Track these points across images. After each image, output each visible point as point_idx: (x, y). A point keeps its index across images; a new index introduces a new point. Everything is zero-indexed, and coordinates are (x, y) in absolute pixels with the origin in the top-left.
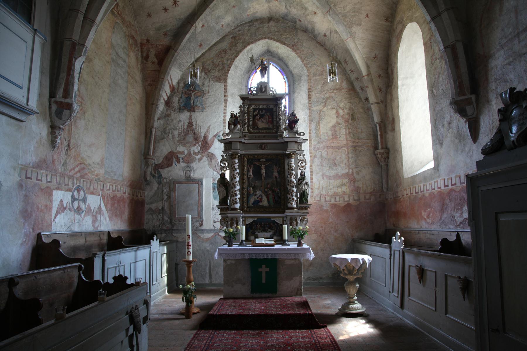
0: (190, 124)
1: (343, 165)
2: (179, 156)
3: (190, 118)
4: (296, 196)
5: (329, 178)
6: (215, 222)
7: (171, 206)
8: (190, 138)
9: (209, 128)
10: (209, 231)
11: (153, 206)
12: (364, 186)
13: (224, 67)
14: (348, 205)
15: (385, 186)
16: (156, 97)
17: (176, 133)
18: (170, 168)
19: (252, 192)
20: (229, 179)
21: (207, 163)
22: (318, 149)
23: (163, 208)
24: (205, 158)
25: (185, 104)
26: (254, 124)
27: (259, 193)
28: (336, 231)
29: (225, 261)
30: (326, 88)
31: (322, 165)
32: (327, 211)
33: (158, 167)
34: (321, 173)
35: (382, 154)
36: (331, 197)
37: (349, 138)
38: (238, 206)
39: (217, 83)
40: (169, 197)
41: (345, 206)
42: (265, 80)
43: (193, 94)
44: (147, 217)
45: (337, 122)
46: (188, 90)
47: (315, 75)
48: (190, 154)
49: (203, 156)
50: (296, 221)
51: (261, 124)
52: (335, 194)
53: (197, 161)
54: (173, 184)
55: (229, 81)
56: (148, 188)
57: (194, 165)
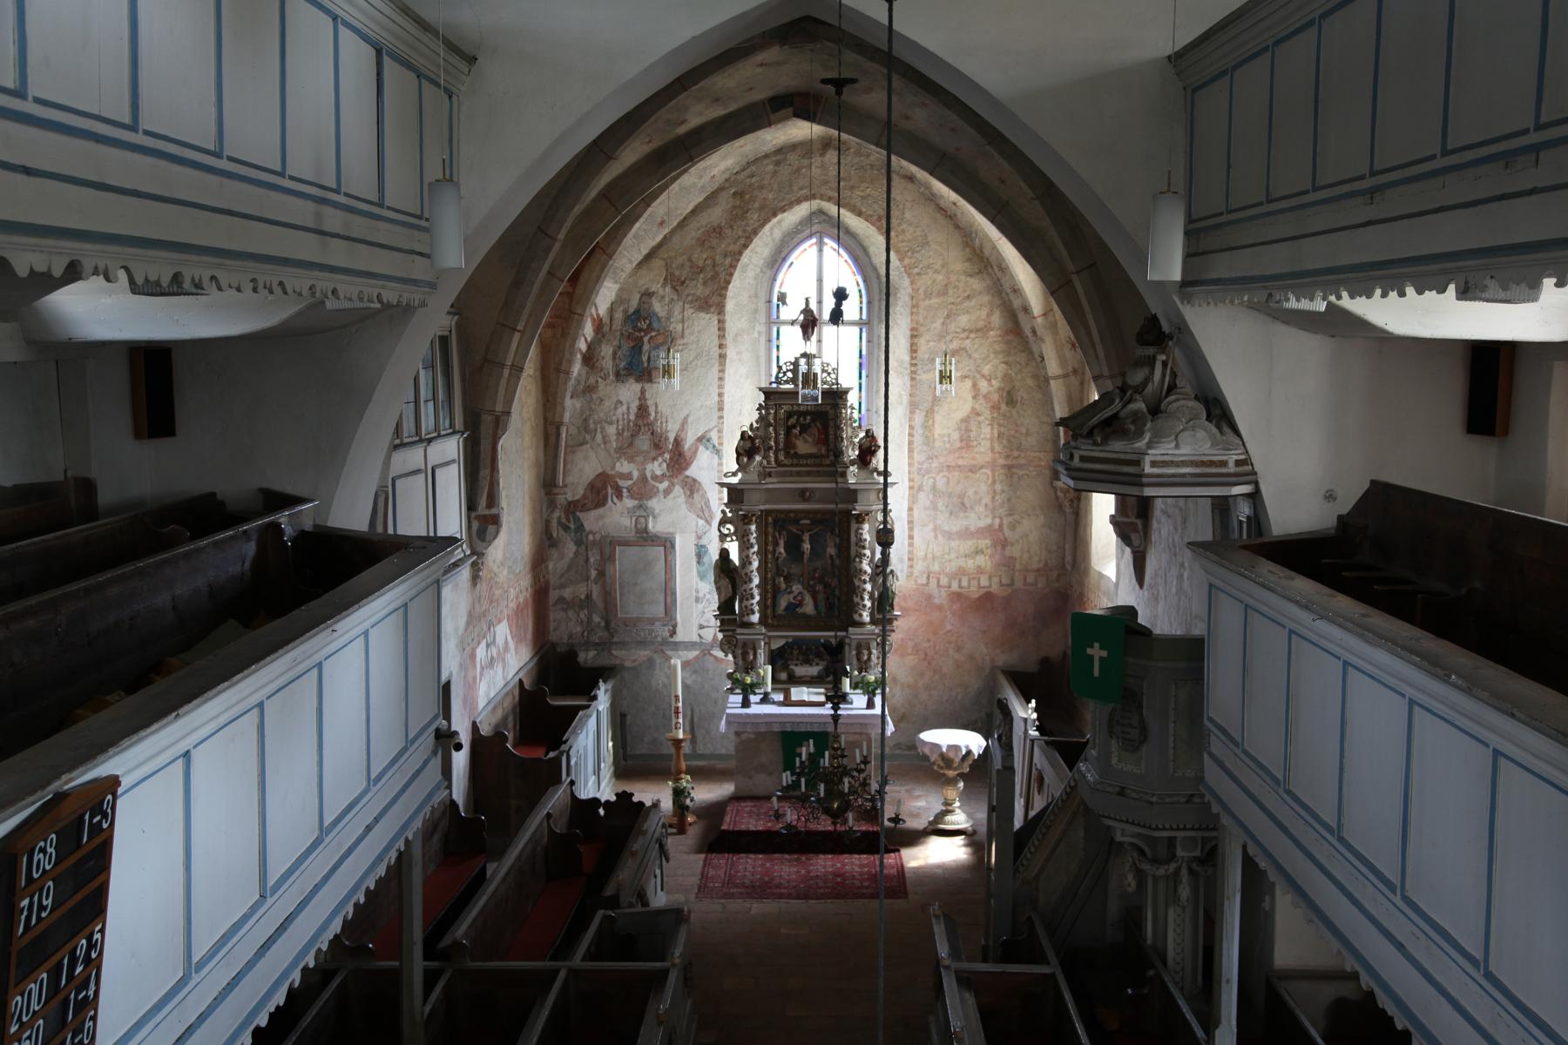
0: (643, 410)
1: (981, 509)
2: (622, 483)
3: (642, 397)
4: (871, 597)
5: (949, 536)
6: (701, 627)
7: (607, 595)
8: (643, 442)
9: (685, 422)
10: (691, 645)
11: (567, 593)
12: (1026, 555)
13: (715, 276)
14: (988, 597)
15: (1068, 558)
16: (567, 355)
17: (612, 430)
18: (600, 511)
19: (783, 586)
20: (737, 562)
21: (682, 499)
22: (928, 472)
23: (589, 597)
24: (678, 490)
25: (630, 364)
26: (789, 445)
27: (797, 588)
28: (959, 649)
29: (737, 734)
30: (952, 327)
31: (935, 508)
32: (940, 608)
33: (573, 508)
34: (931, 526)
35: (1065, 492)
36: (952, 577)
37: (998, 448)
38: (755, 618)
39: (702, 315)
40: (602, 574)
41: (980, 598)
42: (811, 347)
43: (646, 339)
44: (555, 615)
45: (973, 409)
46: (635, 327)
47: (928, 295)
48: (643, 478)
49: (673, 484)
50: (869, 649)
51: (804, 446)
52: (961, 572)
53: (661, 495)
54: (608, 546)
55: (730, 305)
56: (554, 552)
57: (654, 504)
